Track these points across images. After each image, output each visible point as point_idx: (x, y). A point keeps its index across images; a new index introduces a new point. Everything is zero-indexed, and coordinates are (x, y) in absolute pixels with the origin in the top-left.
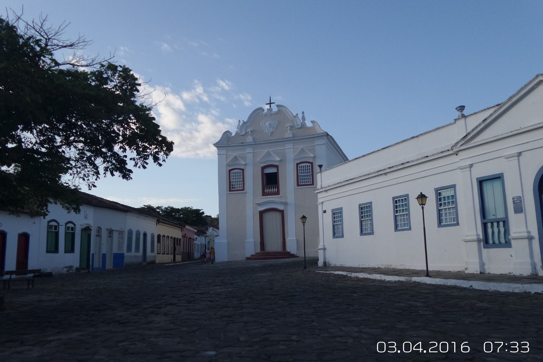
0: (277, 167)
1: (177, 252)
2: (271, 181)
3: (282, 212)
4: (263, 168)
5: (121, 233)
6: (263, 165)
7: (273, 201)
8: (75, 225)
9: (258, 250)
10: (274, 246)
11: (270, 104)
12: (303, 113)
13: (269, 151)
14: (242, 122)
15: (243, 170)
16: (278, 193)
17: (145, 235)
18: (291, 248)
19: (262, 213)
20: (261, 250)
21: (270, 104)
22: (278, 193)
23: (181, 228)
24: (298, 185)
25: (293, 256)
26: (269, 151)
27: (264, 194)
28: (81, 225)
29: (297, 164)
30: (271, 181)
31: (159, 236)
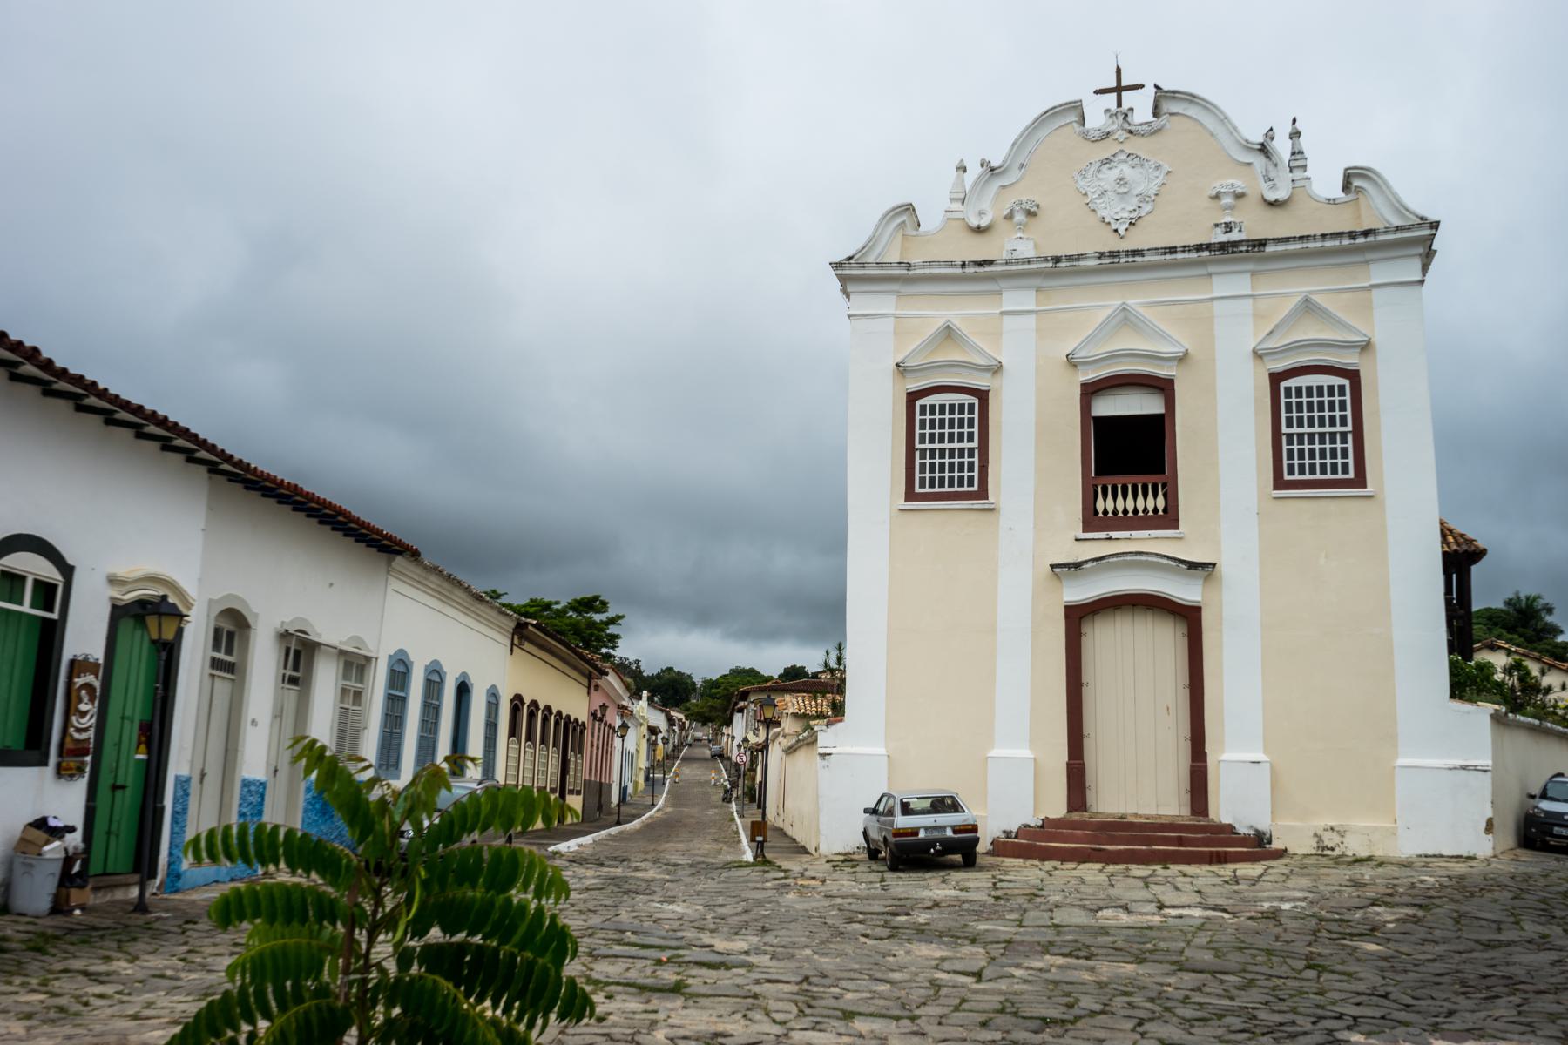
0: (1164, 387)
1: (570, 779)
2: (1130, 453)
3: (1189, 618)
4: (1091, 391)
5: (355, 664)
6: (1091, 375)
7: (1137, 560)
8: (67, 571)
9: (1057, 807)
10: (1140, 786)
11: (1119, 89)
12: (1295, 135)
13: (1124, 309)
14: (974, 171)
15: (983, 396)
16: (1168, 518)
17: (463, 690)
18: (1235, 805)
19: (1078, 617)
20: (1071, 809)
21: (1119, 89)
22: (1168, 518)
23: (590, 677)
24: (1279, 483)
25: (1258, 846)
26: (1124, 309)
27: (1092, 520)
28: (113, 581)
29: (1276, 378)
30: (1130, 453)
31: (517, 702)
